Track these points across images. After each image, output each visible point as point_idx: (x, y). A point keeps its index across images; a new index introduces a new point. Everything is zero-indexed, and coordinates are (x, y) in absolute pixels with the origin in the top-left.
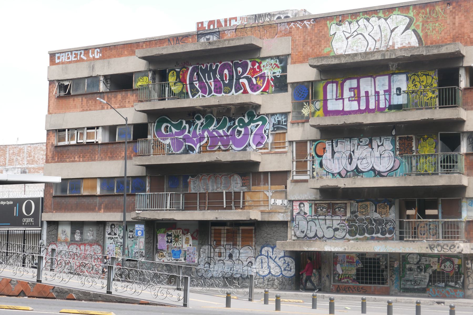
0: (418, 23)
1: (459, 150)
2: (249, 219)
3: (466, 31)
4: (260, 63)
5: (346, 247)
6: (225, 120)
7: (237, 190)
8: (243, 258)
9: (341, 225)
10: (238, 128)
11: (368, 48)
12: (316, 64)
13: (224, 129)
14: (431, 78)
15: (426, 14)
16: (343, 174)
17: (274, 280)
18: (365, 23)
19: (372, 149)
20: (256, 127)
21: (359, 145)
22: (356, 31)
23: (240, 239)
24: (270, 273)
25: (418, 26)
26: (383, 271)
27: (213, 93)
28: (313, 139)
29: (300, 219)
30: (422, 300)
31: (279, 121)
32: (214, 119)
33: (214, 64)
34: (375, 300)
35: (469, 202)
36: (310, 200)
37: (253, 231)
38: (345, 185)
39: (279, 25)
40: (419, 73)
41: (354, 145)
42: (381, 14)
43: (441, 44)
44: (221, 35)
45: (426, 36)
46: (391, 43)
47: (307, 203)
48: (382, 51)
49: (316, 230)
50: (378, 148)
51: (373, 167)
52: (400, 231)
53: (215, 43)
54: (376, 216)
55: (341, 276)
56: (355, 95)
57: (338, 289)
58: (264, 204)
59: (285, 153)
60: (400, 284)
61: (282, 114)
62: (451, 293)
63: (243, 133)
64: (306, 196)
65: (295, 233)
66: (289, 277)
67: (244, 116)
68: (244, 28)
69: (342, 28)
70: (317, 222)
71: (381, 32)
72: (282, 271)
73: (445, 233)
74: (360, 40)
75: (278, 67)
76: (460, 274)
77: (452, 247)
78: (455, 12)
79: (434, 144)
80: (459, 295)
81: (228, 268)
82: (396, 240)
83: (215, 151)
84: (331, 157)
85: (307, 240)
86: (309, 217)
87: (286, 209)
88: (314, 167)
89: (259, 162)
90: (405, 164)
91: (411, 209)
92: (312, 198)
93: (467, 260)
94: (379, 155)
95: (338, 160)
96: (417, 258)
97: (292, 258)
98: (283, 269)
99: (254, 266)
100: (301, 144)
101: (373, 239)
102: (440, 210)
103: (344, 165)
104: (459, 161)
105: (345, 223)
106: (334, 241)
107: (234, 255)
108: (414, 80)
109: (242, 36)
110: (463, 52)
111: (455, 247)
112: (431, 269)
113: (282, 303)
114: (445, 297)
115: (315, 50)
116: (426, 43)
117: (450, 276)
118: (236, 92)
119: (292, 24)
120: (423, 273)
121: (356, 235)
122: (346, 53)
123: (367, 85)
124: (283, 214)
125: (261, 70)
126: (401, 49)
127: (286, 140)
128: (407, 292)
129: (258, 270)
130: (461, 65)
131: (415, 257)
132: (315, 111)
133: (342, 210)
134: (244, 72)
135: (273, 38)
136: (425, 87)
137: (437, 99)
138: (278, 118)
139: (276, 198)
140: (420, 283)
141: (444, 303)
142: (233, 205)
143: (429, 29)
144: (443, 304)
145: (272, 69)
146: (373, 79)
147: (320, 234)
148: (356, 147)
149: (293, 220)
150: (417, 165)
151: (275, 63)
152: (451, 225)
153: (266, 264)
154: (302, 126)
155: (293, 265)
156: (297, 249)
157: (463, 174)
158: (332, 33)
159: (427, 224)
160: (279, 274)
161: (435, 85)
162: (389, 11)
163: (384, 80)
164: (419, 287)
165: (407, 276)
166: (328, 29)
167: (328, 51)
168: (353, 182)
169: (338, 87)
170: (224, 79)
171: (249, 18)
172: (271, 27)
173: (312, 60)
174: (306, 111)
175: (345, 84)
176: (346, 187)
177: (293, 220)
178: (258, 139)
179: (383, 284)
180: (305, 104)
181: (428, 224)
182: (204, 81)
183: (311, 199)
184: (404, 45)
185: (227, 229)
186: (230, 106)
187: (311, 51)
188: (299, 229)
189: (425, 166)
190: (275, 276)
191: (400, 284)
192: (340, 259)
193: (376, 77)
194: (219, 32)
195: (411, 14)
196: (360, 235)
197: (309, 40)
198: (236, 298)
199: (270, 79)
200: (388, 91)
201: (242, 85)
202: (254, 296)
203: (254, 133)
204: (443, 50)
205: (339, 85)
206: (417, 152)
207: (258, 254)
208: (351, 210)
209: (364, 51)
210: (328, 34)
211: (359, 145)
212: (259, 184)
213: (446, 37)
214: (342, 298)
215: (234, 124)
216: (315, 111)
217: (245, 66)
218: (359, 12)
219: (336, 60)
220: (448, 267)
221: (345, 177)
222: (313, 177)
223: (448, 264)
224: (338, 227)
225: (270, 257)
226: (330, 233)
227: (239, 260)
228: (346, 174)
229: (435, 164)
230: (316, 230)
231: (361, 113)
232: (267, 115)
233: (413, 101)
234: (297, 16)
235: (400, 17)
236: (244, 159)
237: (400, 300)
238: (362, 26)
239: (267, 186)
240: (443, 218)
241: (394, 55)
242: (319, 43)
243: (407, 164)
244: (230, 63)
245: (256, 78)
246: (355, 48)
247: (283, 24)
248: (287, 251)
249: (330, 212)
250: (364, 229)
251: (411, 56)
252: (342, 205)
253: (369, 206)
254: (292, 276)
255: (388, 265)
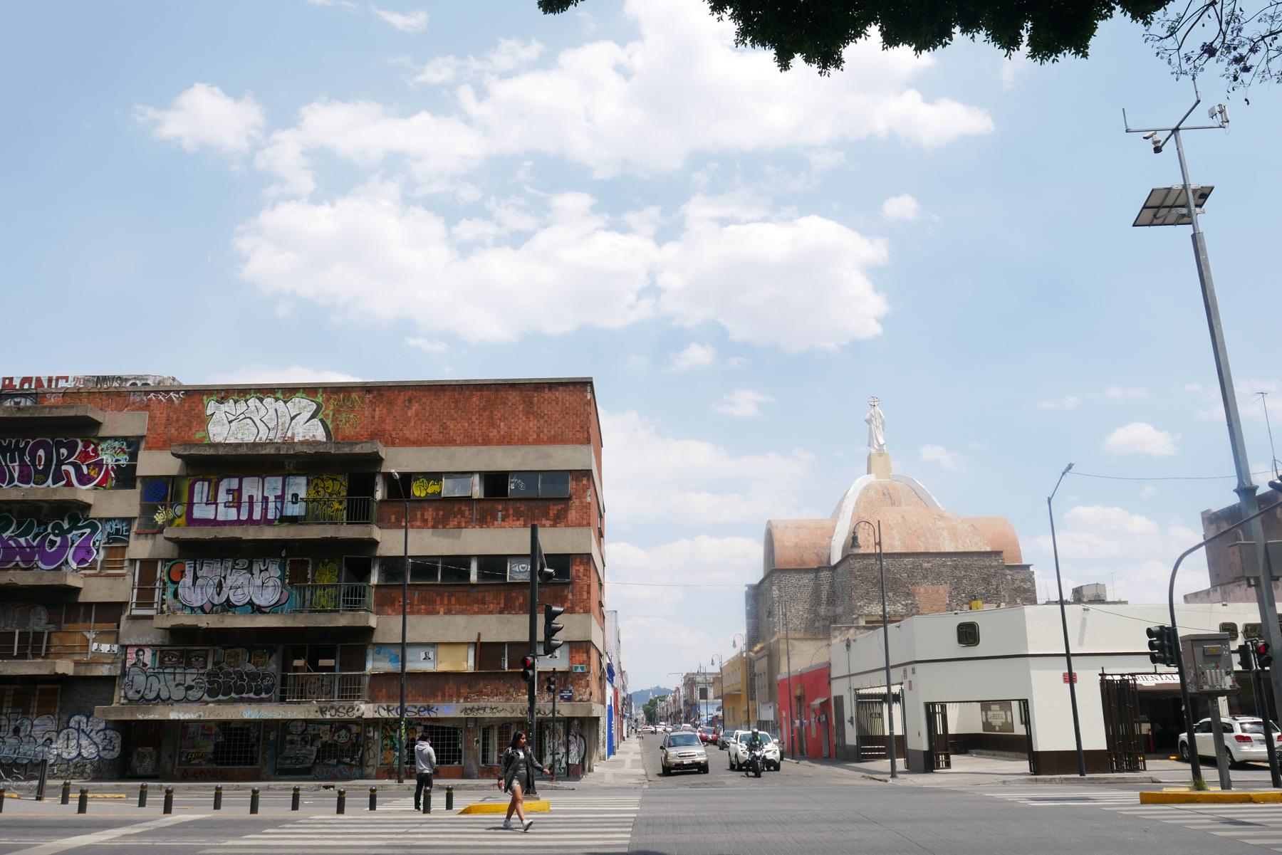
0: (327, 412)
1: (369, 580)
2: (53, 673)
3: (387, 428)
4: (97, 445)
5: (201, 713)
6: (31, 524)
7: (38, 629)
8: (38, 733)
9: (197, 681)
10: (51, 537)
11: (258, 437)
12: (180, 453)
13: (28, 537)
14: (339, 484)
15: (339, 401)
16: (207, 609)
17: (86, 765)
18: (257, 405)
19: (252, 574)
20: (80, 536)
21: (233, 568)
22: (243, 413)
23: (36, 704)
24: (80, 754)
25: (327, 415)
26: (253, 746)
27: (16, 483)
28: (167, 557)
29: (136, 673)
30: (303, 785)
31: (117, 530)
32: (13, 521)
33: (23, 440)
34: (238, 788)
35: (376, 649)
36: (153, 646)
37: (59, 691)
38: (208, 623)
39: (132, 394)
40: (325, 477)
41: (226, 569)
42: (279, 395)
43: (355, 441)
44: (38, 400)
45: (337, 429)
46: (289, 434)
47: (148, 649)
48: (277, 443)
49: (160, 689)
50: (260, 573)
51: (251, 599)
52: (281, 689)
53: (28, 410)
54: (250, 668)
55: (192, 756)
56: (233, 499)
57: (185, 775)
58: (81, 650)
59: (123, 575)
60: (276, 764)
61: (123, 520)
62: (344, 773)
63: (58, 544)
64: (148, 639)
65: (125, 693)
66: (110, 760)
67: (63, 520)
68: (78, 392)
69: (225, 407)
70: (161, 677)
71: (278, 418)
72: (99, 751)
73: (342, 691)
74: (248, 426)
75: (125, 453)
76: (358, 746)
77: (350, 710)
78: (375, 403)
79: (337, 572)
80: (355, 774)
81: (10, 750)
82: (275, 702)
83: (9, 569)
84: (191, 584)
85: (144, 704)
86: (149, 670)
87: (115, 658)
88: (164, 597)
89: (80, 589)
90: (296, 596)
91: (299, 658)
92: (157, 641)
93: (369, 727)
94: (261, 584)
95: (202, 589)
96: (302, 726)
97: (117, 731)
98: (101, 749)
99: (54, 746)
100: (148, 565)
101: (242, 700)
102: (338, 660)
103: (209, 596)
104: (367, 594)
105: (203, 678)
106: (185, 704)
107: (22, 728)
108: (317, 485)
109: (72, 404)
110: (383, 454)
111: (353, 709)
112: (320, 740)
113: (91, 801)
114: (336, 779)
115: (183, 434)
116: (336, 438)
117: (346, 748)
118: (54, 484)
119: (152, 394)
120: (308, 747)
121: (218, 695)
122: (227, 442)
123: (253, 488)
124: (109, 666)
125: (97, 455)
126: (302, 443)
127: (126, 558)
128: (285, 774)
129: (60, 751)
130: (378, 471)
131: (299, 724)
132: (174, 518)
133: (201, 659)
134: (70, 455)
135: (121, 410)
136: (330, 495)
137: (345, 512)
138: (116, 525)
139: (101, 642)
140: (303, 760)
141: (333, 787)
142: (29, 651)
143: (341, 421)
144: (332, 789)
145: (114, 454)
146: (261, 480)
147: (164, 695)
148: (229, 571)
149: (124, 674)
150: (312, 599)
151: (120, 446)
152: (351, 680)
153: (75, 741)
154: (152, 539)
155: (118, 743)
156: (127, 717)
157: (371, 612)
158: (209, 412)
159: (318, 679)
160: (93, 756)
161: (344, 494)
162: (290, 393)
163: (276, 482)
164: (301, 766)
165: (287, 751)
166: (204, 407)
167: (201, 436)
168: (221, 620)
169: (211, 488)
170: (37, 463)
171: (88, 380)
172: (119, 396)
173: (176, 447)
174: (159, 518)
175: (221, 483)
176: (210, 626)
177: (124, 674)
178: (82, 554)
179: (252, 764)
180: (160, 508)
181: (321, 678)
182: (4, 464)
183: (156, 643)
184: (307, 438)
185: (15, 689)
186: (43, 504)
187: (176, 433)
188: (134, 687)
189: (322, 600)
190: (87, 759)
191: (276, 764)
192: (191, 730)
193: (265, 478)
194: (36, 394)
195: (320, 399)
196: (223, 695)
197: (175, 418)
198: (16, 796)
199: (110, 467)
200: (280, 498)
201: (65, 473)
202: (46, 792)
203: (76, 545)
204: (357, 449)
205: (213, 484)
206: (313, 581)
207: (64, 726)
208: (214, 660)
209: (252, 441)
210: (204, 414)
211: (233, 568)
212: (75, 621)
213: (362, 433)
214: (189, 788)
215: (46, 530)
216: (174, 518)
217: (72, 449)
218: (250, 389)
219: (212, 450)
220: (343, 737)
221: (209, 613)
222: (162, 612)
223: (343, 732)
224: (193, 684)
225: (83, 731)
226: (179, 693)
227: (30, 736)
228: (212, 609)
229: (336, 597)
230: (160, 689)
231: (240, 525)
232: (100, 520)
233: (313, 512)
234: (162, 385)
235: (305, 402)
236: (56, 583)
237: (273, 787)
238: (253, 408)
239: (88, 624)
240: (341, 670)
241: (292, 450)
242: (189, 425)
243: (298, 597)
244: (49, 440)
245: (88, 466)
246: (240, 436)
247: (139, 393)
248: (111, 721)
249: (182, 663)
250: (230, 687)
251: (315, 453)
252: (204, 653)
253: (241, 655)
254: (115, 759)
255: (261, 737)
